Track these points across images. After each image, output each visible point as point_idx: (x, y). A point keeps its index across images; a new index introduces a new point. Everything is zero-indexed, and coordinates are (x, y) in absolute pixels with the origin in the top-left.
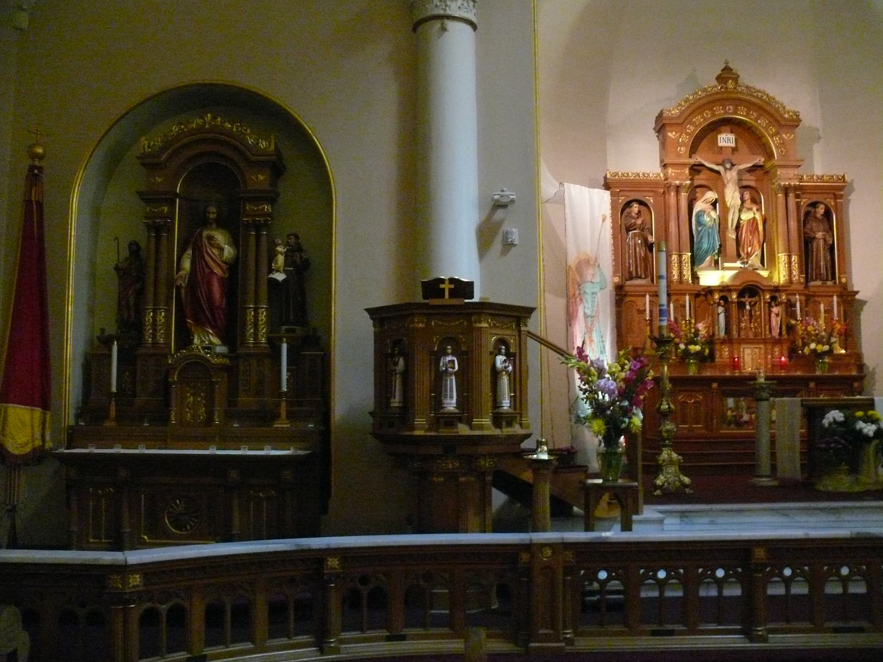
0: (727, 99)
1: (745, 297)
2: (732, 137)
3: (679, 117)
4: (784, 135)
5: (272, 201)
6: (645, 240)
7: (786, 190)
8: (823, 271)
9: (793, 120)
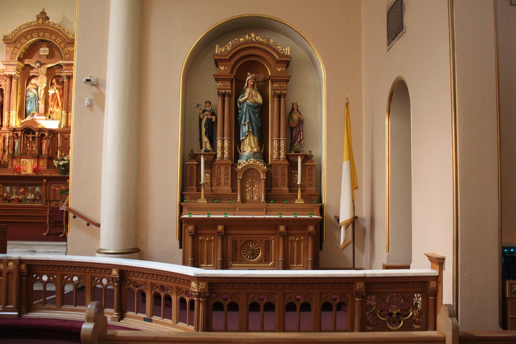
0: (40, 29)
1: (30, 134)
2: (47, 49)
4: (69, 48)
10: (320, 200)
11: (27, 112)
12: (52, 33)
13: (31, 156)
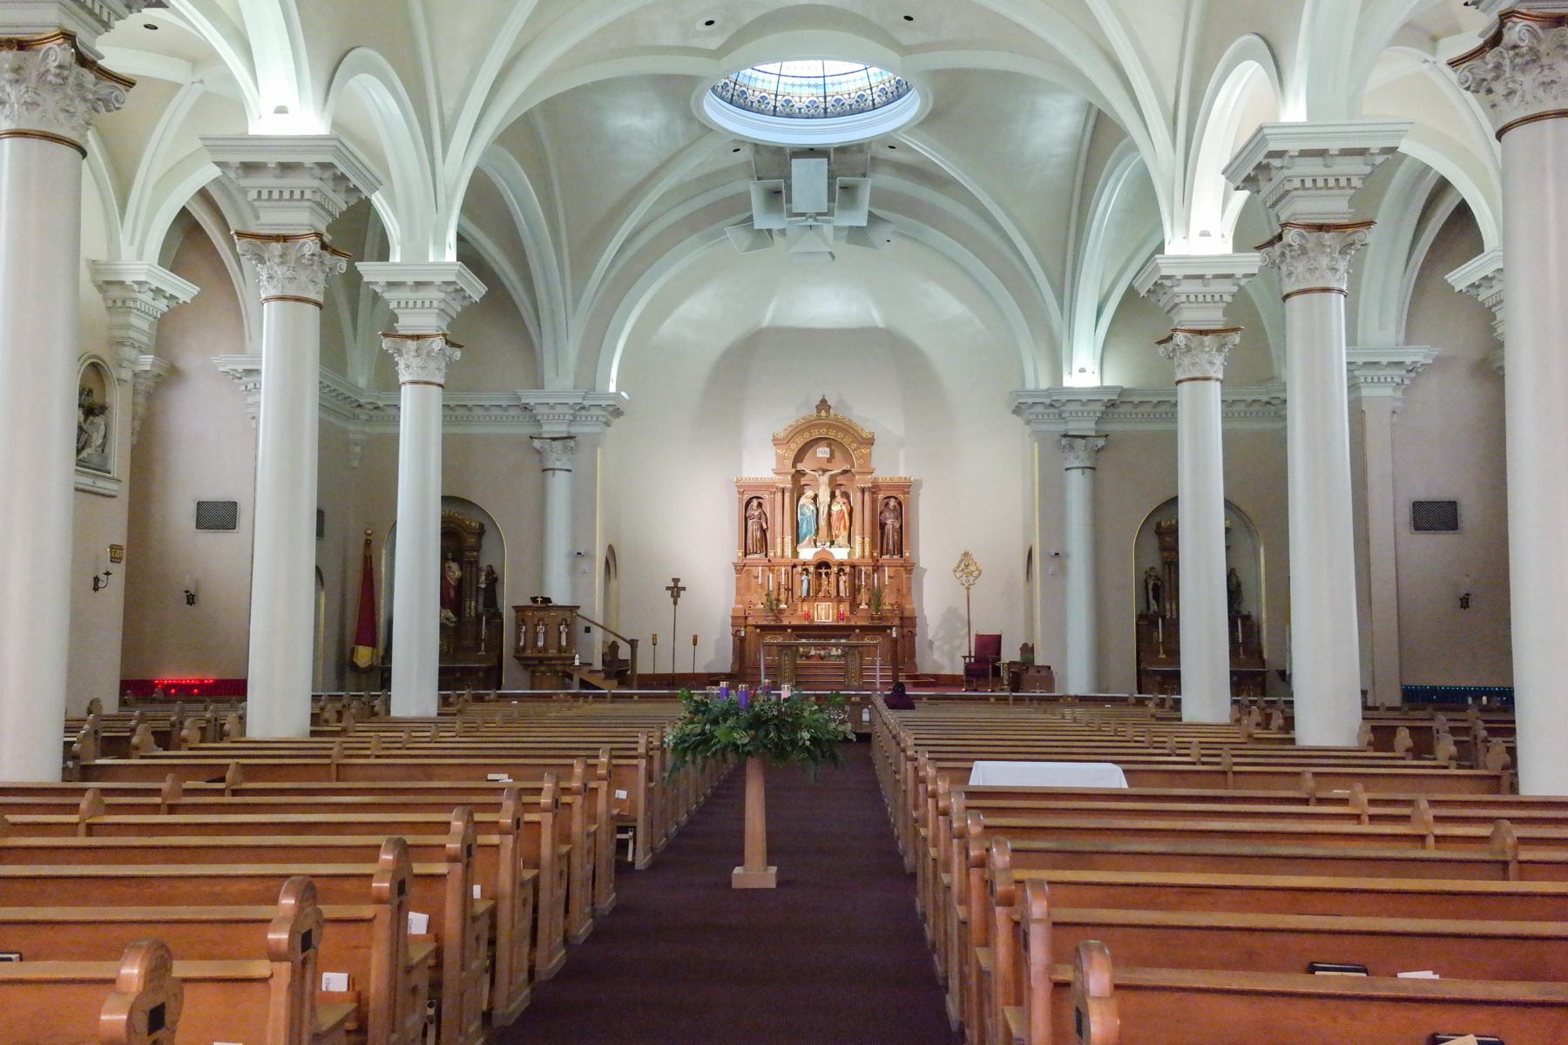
2: (828, 449)
3: (784, 439)
5: (478, 551)
6: (762, 526)
7: (863, 491)
8: (891, 547)
9: (869, 439)
10: (1261, 654)
11: (801, 534)
12: (839, 429)
13: (827, 598)
